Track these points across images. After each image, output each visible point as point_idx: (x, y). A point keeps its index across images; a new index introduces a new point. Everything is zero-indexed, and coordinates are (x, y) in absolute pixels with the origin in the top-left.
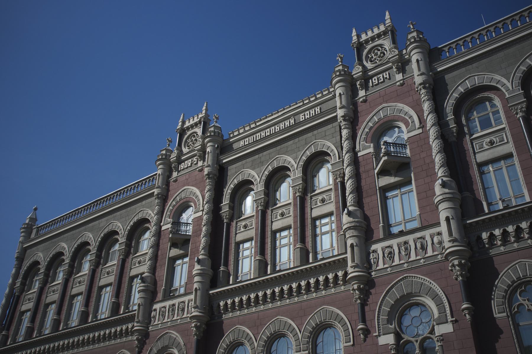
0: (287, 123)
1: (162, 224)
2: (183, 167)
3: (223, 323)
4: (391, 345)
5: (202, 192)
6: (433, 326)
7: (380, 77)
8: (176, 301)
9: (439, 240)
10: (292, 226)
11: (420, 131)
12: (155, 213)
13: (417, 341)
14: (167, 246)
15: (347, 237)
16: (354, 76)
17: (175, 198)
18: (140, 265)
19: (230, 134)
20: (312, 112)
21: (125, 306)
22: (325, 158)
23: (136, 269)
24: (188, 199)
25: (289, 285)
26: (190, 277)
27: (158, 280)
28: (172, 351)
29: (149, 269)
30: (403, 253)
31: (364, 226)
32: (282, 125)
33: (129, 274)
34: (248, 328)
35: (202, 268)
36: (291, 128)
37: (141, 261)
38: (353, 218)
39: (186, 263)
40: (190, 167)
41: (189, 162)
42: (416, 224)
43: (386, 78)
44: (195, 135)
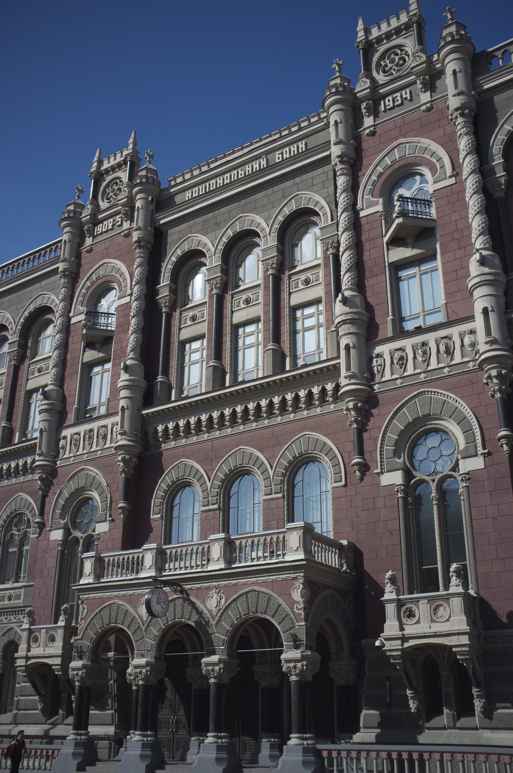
0: (256, 166)
1: (71, 314)
2: (100, 229)
3: (162, 455)
4: (397, 486)
5: (129, 267)
6: (457, 461)
7: (397, 96)
8: (94, 425)
9: (471, 341)
10: (262, 319)
11: (453, 180)
12: (60, 298)
13: (433, 481)
14: (79, 347)
15: (340, 334)
16: (358, 95)
17: (90, 276)
18: (41, 374)
19: (170, 181)
20: (294, 148)
21: (20, 432)
22: (312, 218)
23: (36, 379)
24: (108, 278)
25: (256, 402)
26: (114, 391)
27: (67, 396)
28: (90, 494)
29: (53, 379)
30: (420, 359)
31: (365, 319)
32: (248, 169)
33: (26, 387)
34: (197, 462)
35: (132, 377)
36: (262, 172)
38: (350, 308)
39: (108, 371)
40: (111, 230)
41: (109, 223)
42: (440, 318)
44: (118, 181)
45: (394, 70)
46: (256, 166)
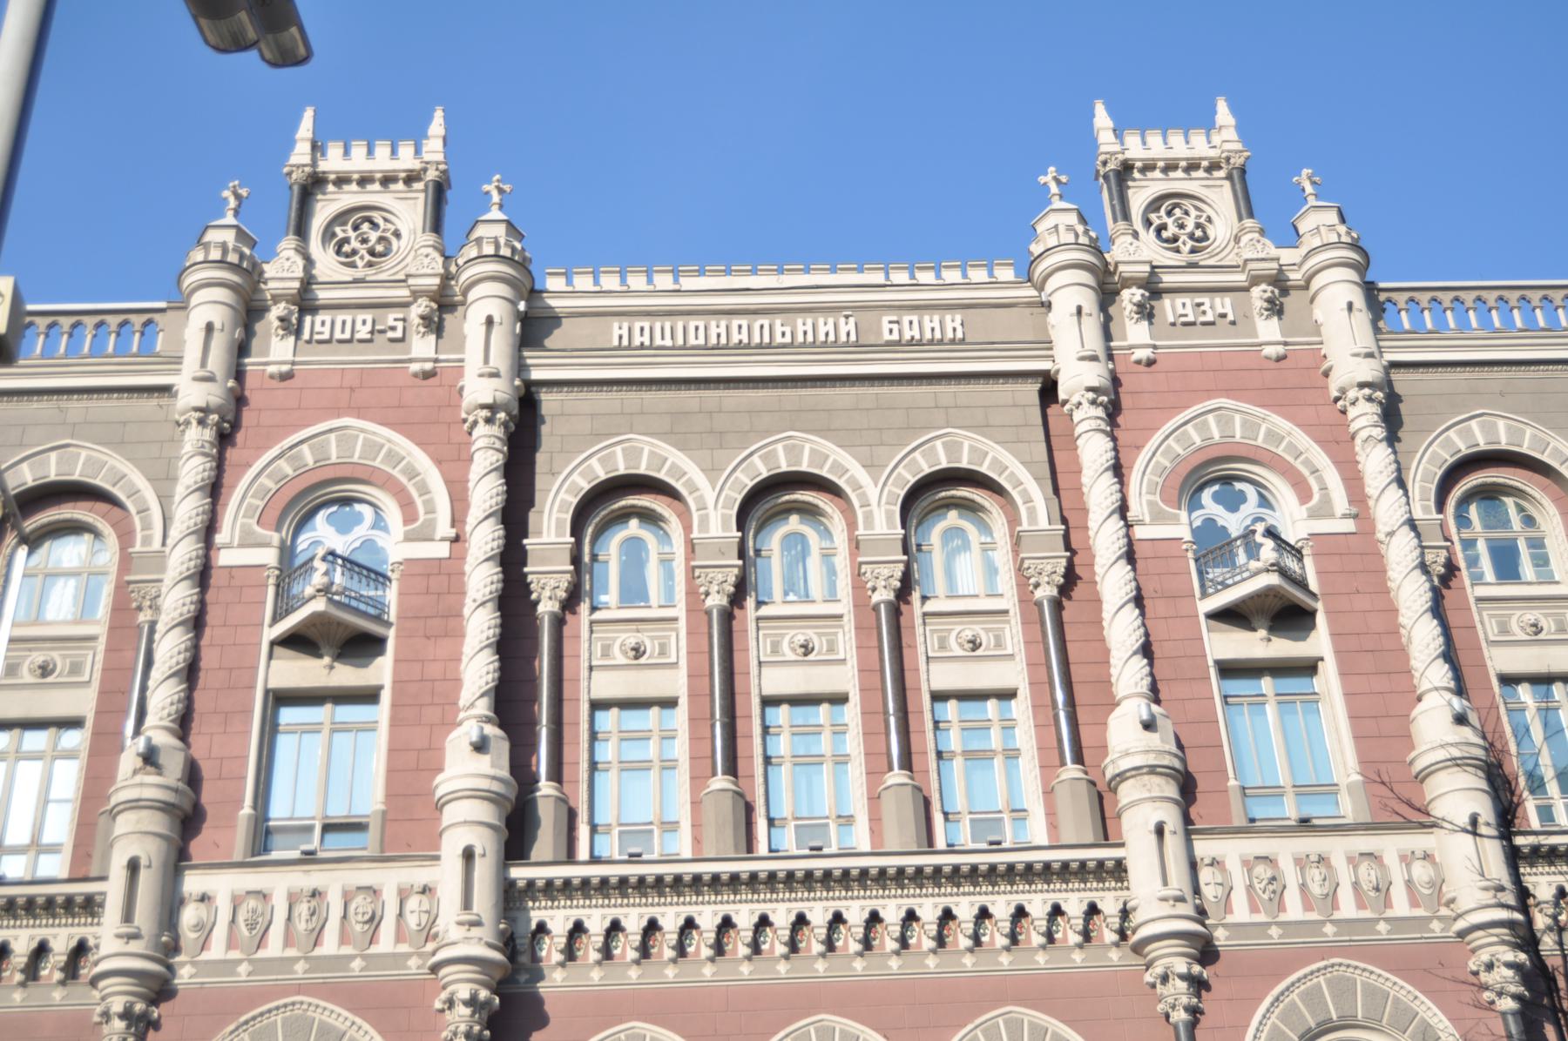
1: (219, 539)
7: (1202, 304)
11: (1349, 526)
17: (291, 448)
23: (25, 693)
32: (803, 325)
37: (55, 666)
43: (1223, 316)
45: (1184, 244)
46: (825, 326)
